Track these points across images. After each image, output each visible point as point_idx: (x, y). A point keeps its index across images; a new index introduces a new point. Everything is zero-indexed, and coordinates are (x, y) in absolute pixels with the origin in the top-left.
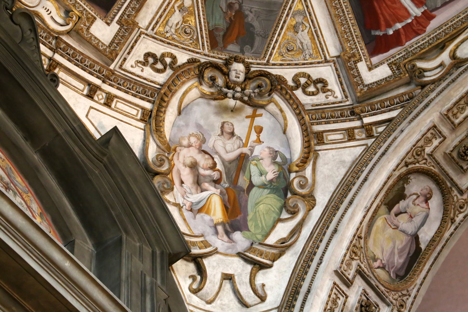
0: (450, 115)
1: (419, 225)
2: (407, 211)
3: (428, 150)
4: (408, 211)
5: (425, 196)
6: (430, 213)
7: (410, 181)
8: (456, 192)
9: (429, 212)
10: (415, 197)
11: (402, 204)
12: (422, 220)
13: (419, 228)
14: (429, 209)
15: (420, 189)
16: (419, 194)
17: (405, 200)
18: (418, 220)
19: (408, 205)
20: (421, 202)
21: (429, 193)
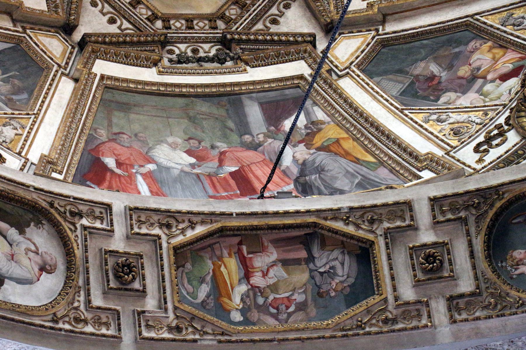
0: (134, 217)
1: (14, 276)
2: (13, 246)
3: (85, 222)
4: (14, 247)
5: (45, 263)
6: (36, 284)
7: (41, 229)
8: (82, 298)
9: (35, 282)
10: (33, 248)
11: (13, 233)
12: (21, 277)
13: (11, 279)
14: (38, 280)
15: (46, 250)
16: (40, 252)
17: (20, 234)
18: (17, 271)
19: (19, 243)
20: (36, 262)
21: (50, 266)
